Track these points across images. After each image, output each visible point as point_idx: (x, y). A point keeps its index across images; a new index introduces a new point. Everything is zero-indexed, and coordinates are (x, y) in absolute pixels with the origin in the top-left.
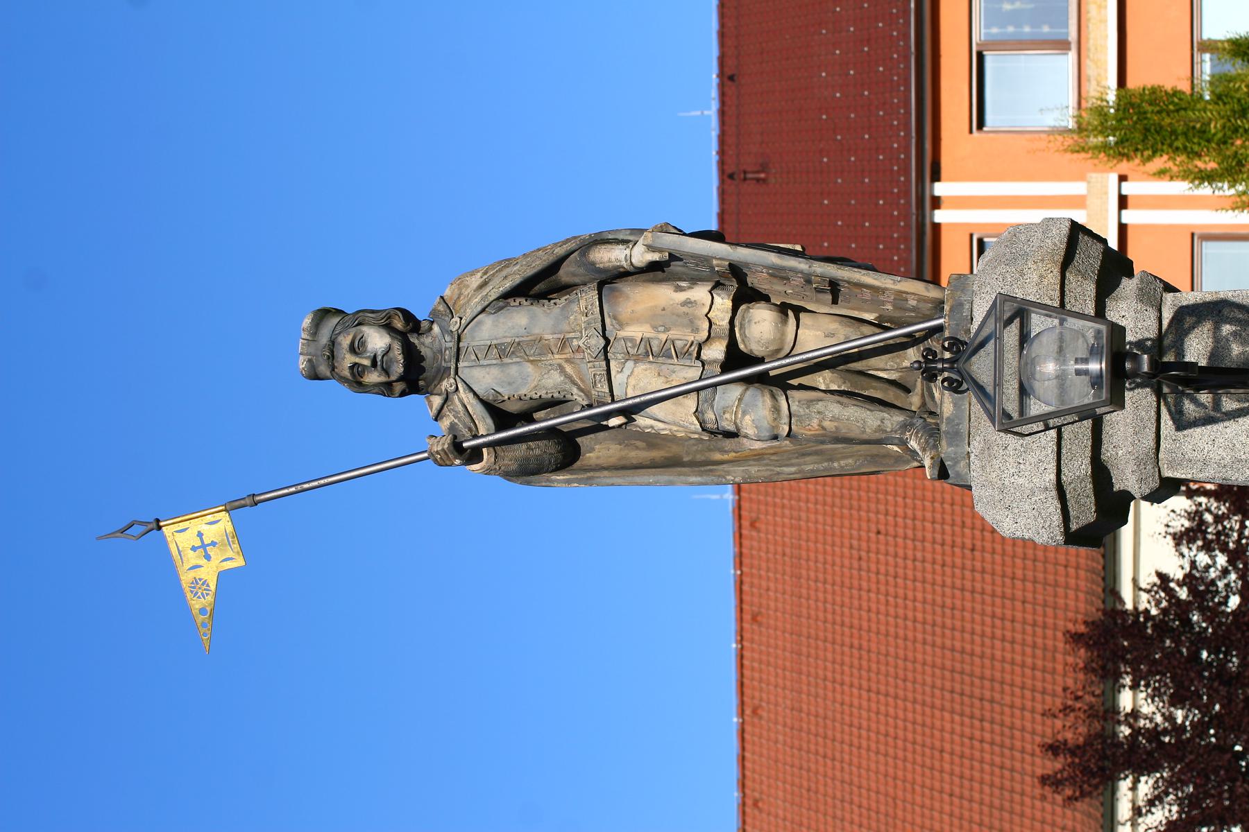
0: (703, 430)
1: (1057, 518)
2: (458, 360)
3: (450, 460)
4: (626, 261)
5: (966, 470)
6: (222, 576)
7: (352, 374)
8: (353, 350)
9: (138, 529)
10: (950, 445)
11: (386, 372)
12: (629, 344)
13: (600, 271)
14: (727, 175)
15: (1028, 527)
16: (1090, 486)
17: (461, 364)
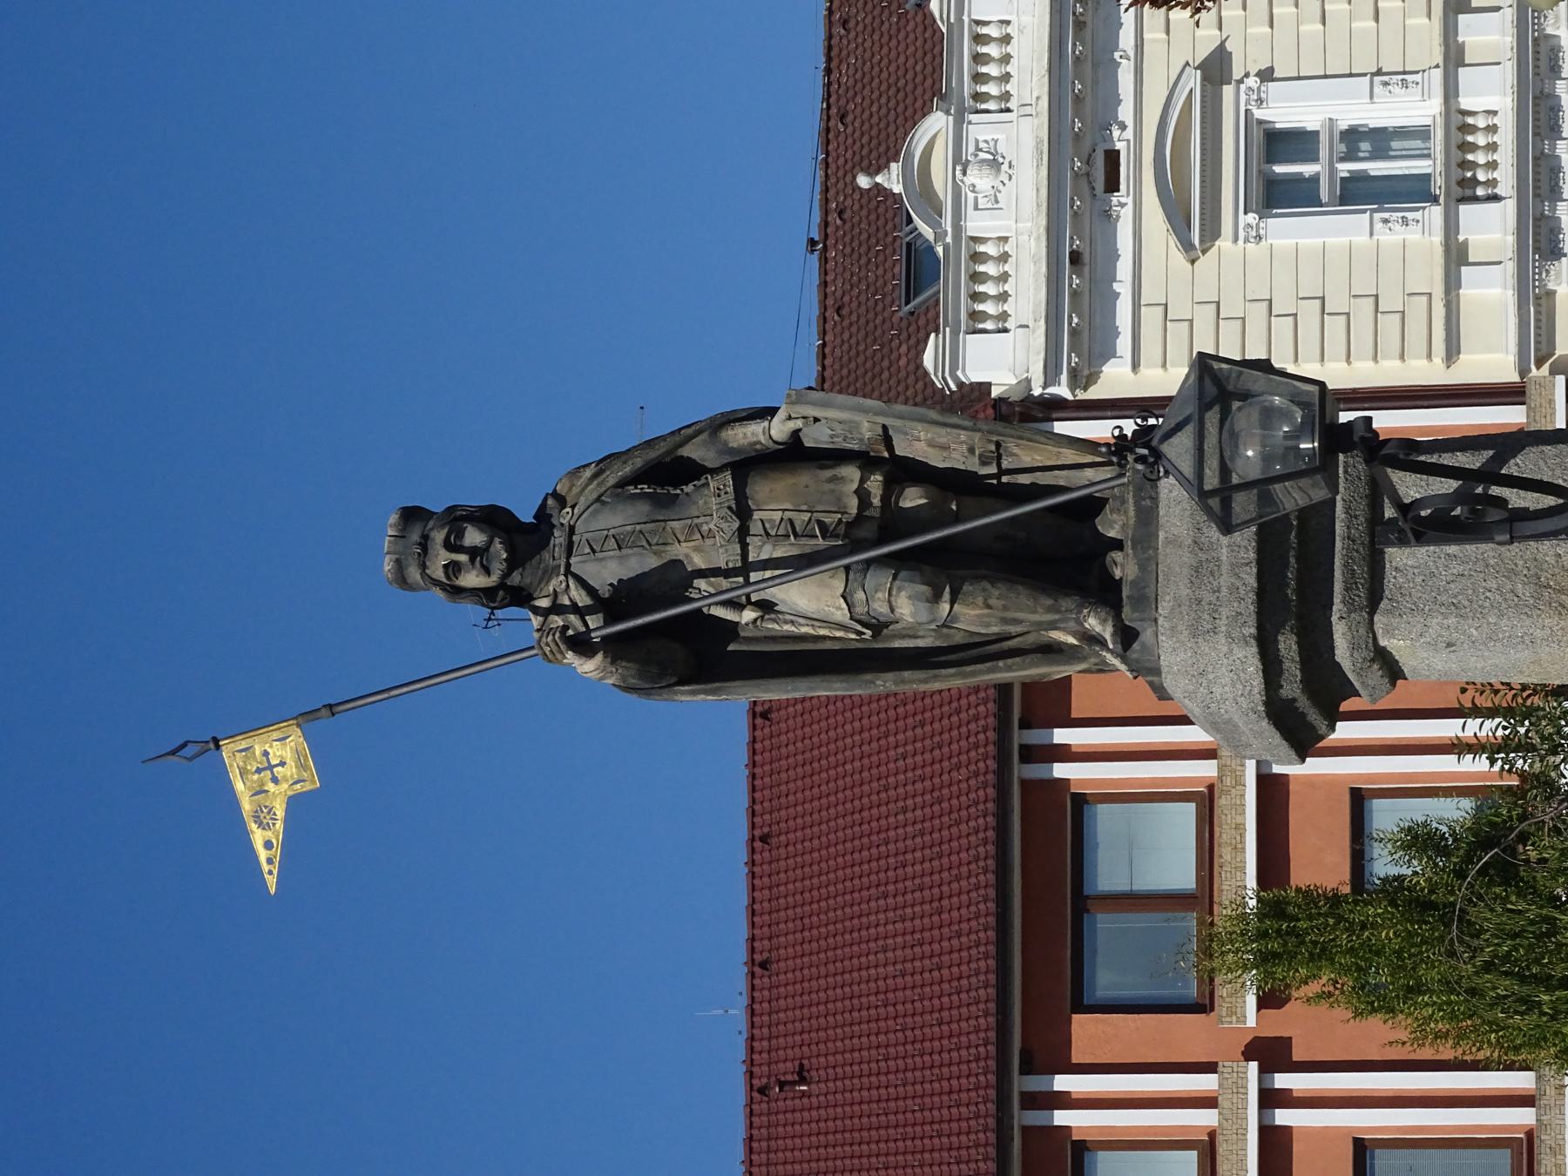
0: (851, 618)
2: (569, 554)
3: (561, 652)
4: (764, 433)
5: (1153, 641)
6: (294, 802)
9: (190, 750)
10: (1134, 611)
12: (767, 525)
13: (732, 451)
14: (758, 1091)
15: (1225, 697)
16: (1295, 647)
17: (573, 560)
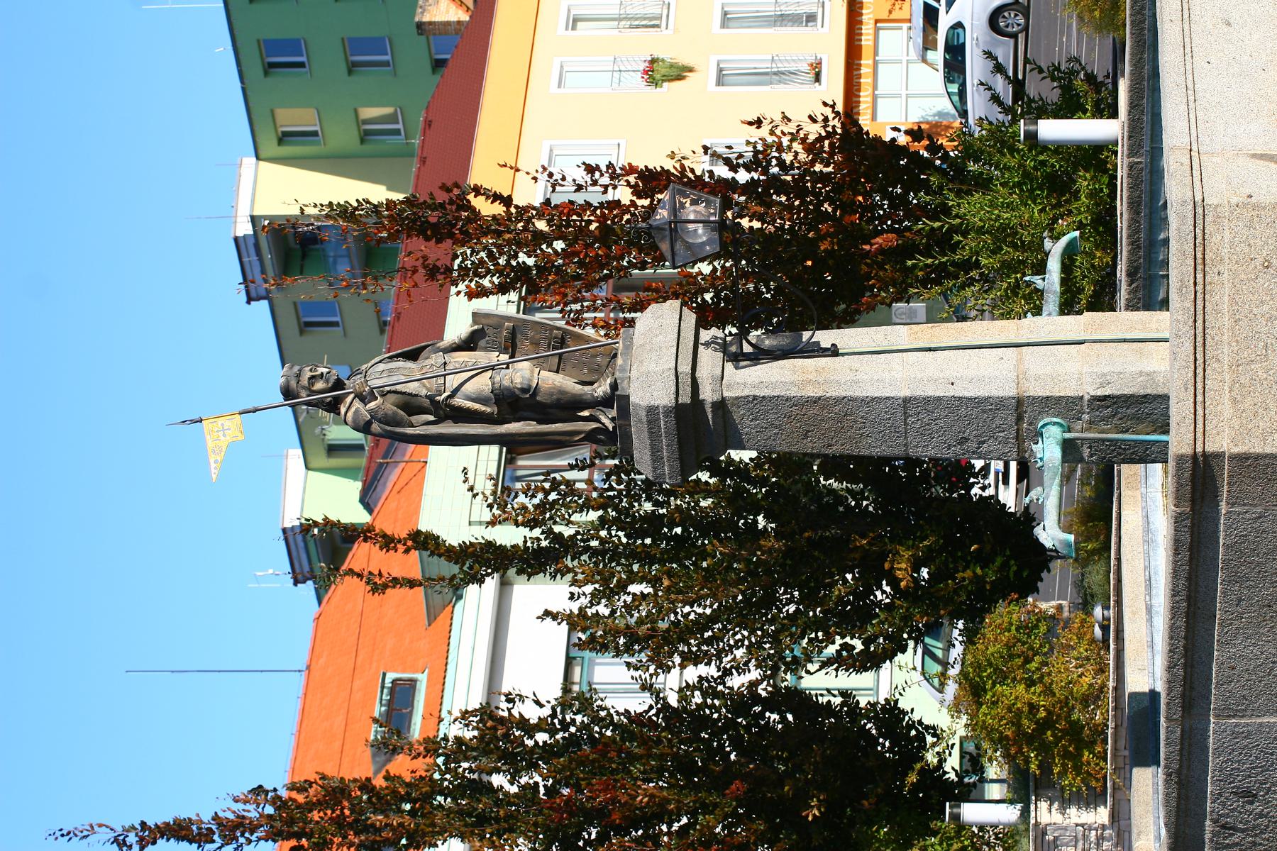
1: (673, 388)
7: (309, 383)
8: (311, 370)
11: (327, 381)
